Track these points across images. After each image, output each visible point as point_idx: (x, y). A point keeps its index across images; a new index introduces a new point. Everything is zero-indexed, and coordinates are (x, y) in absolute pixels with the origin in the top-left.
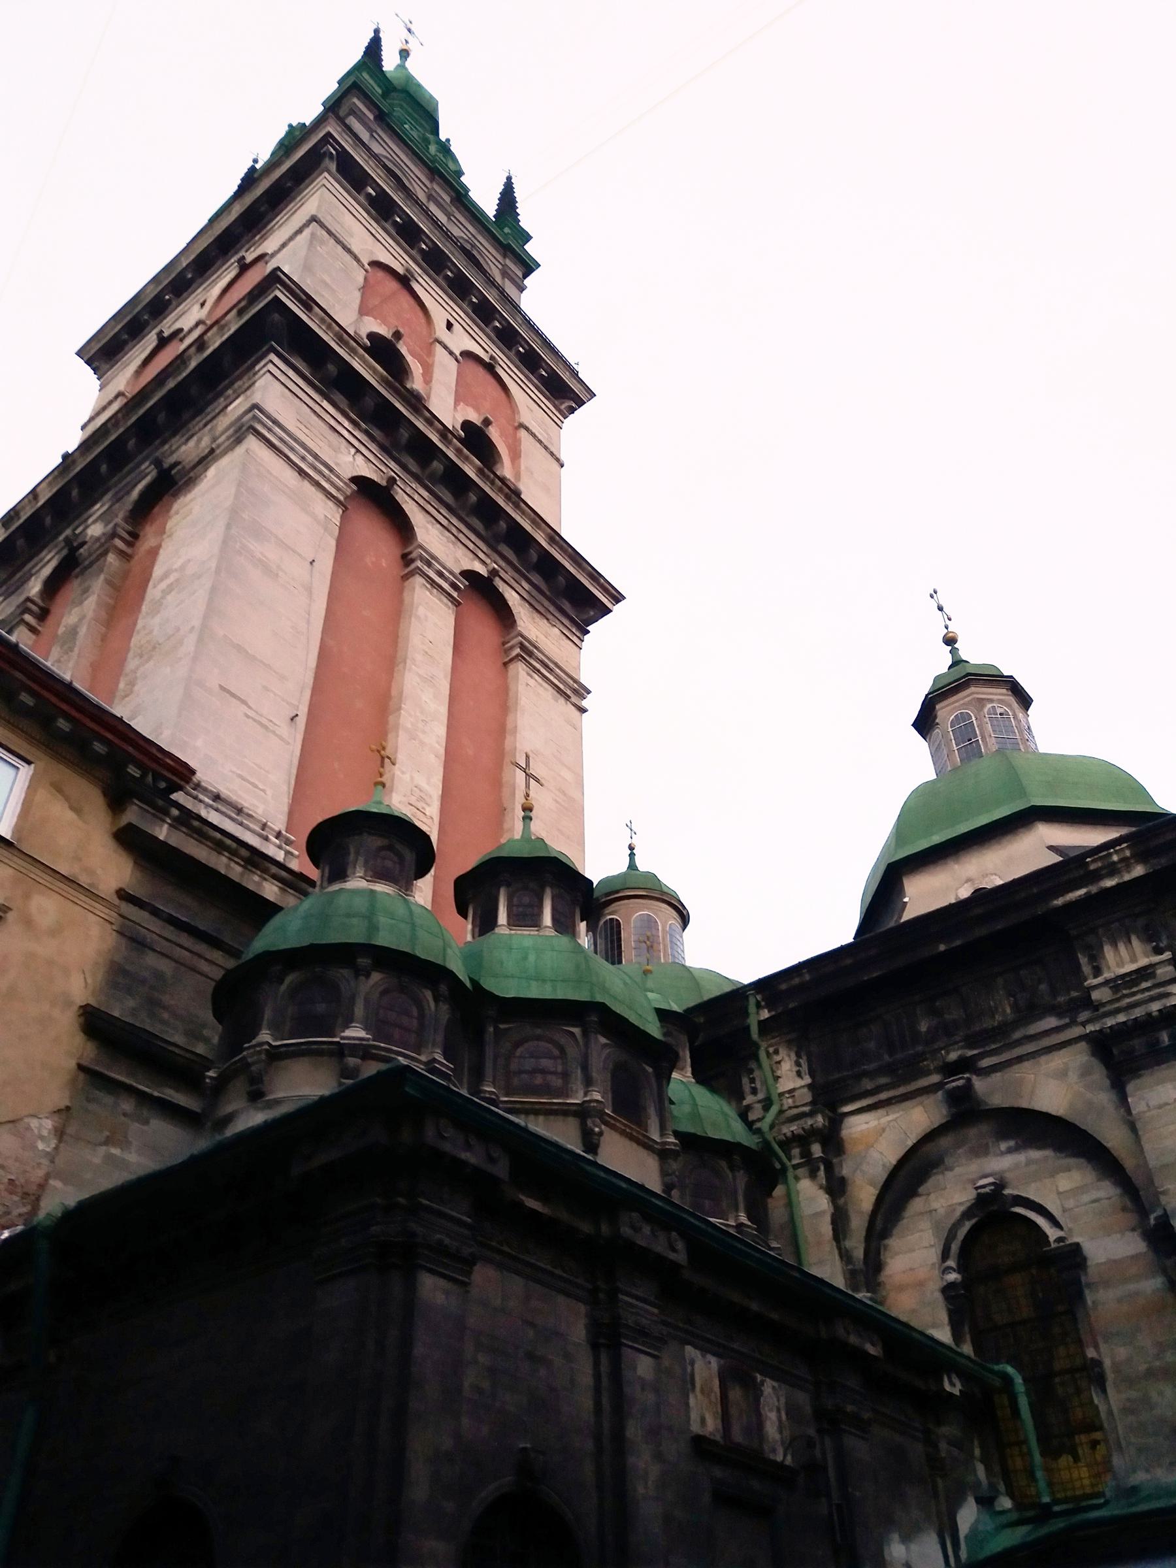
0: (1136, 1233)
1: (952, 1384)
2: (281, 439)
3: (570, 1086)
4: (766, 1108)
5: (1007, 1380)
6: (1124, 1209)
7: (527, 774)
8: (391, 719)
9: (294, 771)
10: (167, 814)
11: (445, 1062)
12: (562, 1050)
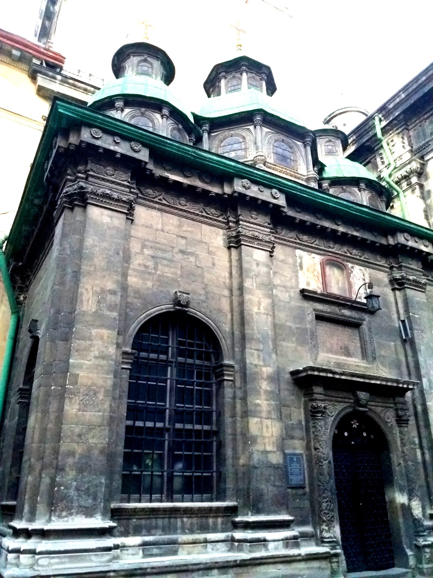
3: (248, 153)
10: (55, 78)
12: (244, 138)
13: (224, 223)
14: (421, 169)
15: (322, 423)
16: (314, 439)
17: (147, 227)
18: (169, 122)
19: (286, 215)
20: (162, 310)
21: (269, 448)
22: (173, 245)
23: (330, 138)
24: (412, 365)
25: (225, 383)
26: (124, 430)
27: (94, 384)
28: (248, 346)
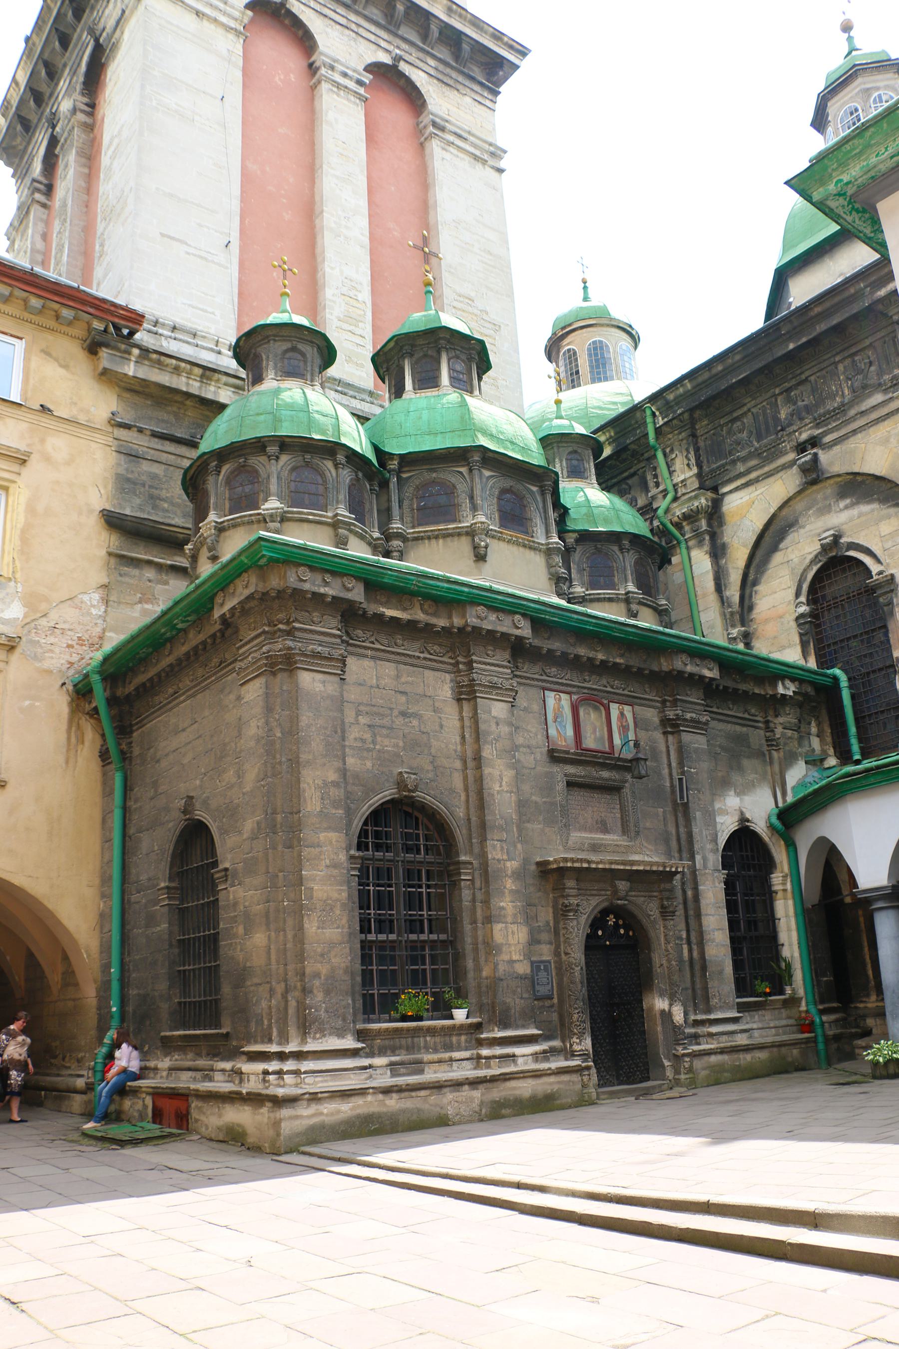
1: (785, 687)
4: (665, 497)
5: (836, 679)
8: (317, 221)
9: (236, 291)
10: (130, 353)
11: (348, 514)
12: (454, 486)
13: (451, 664)
14: (713, 508)
15: (575, 923)
16: (565, 942)
17: (360, 684)
18: (345, 472)
20: (386, 796)
21: (515, 957)
22: (393, 706)
23: (575, 447)
24: (683, 837)
25: (463, 883)
26: (359, 946)
27: (329, 898)
28: (489, 836)
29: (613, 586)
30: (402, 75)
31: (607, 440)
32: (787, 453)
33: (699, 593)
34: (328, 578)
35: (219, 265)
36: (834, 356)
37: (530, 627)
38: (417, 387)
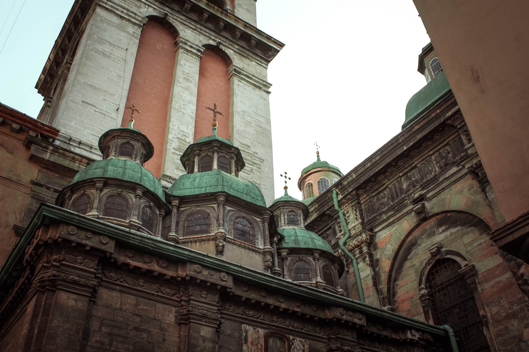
0: (497, 255)
1: (412, 335)
2: (112, 6)
5: (446, 331)
6: (492, 245)
7: (214, 112)
10: (48, 149)
12: (209, 214)
14: (370, 240)
17: (107, 307)
19: (233, 294)
23: (292, 208)
29: (310, 279)
30: (221, 50)
31: (314, 210)
32: (408, 206)
33: (364, 287)
34: (89, 235)
35: (112, 118)
36: (429, 151)
37: (232, 281)
38: (200, 170)
